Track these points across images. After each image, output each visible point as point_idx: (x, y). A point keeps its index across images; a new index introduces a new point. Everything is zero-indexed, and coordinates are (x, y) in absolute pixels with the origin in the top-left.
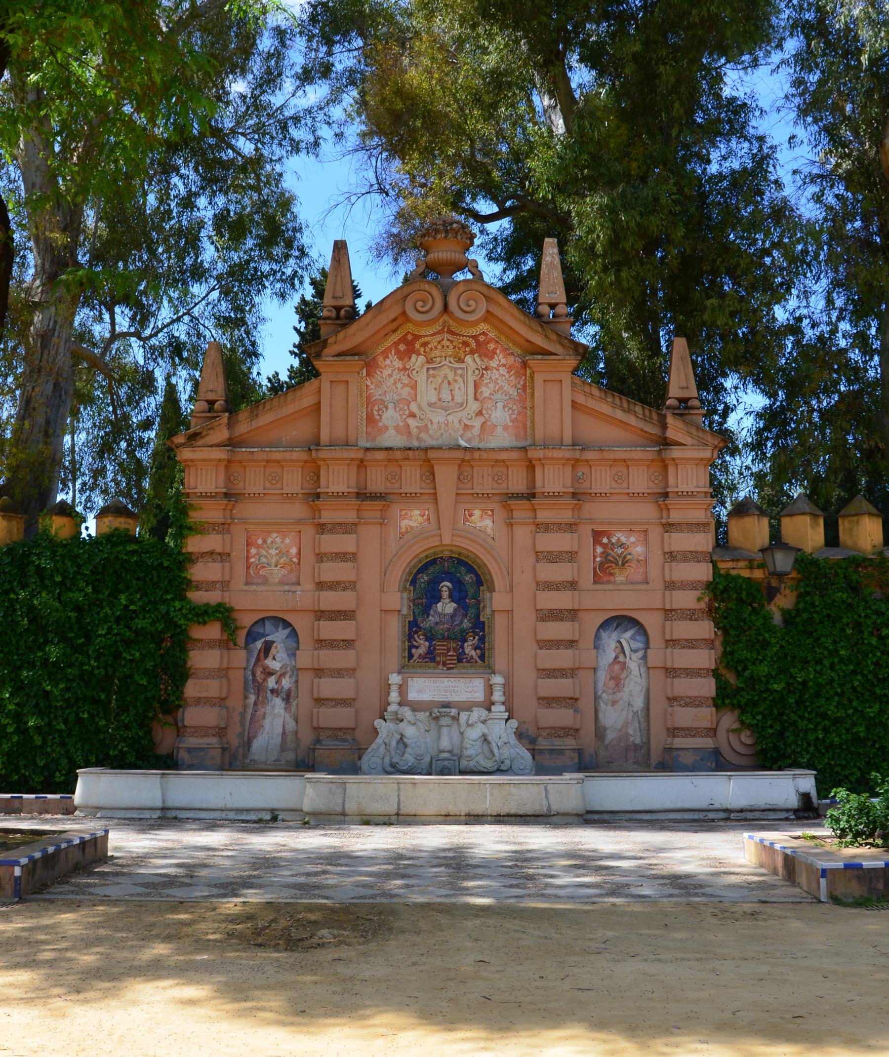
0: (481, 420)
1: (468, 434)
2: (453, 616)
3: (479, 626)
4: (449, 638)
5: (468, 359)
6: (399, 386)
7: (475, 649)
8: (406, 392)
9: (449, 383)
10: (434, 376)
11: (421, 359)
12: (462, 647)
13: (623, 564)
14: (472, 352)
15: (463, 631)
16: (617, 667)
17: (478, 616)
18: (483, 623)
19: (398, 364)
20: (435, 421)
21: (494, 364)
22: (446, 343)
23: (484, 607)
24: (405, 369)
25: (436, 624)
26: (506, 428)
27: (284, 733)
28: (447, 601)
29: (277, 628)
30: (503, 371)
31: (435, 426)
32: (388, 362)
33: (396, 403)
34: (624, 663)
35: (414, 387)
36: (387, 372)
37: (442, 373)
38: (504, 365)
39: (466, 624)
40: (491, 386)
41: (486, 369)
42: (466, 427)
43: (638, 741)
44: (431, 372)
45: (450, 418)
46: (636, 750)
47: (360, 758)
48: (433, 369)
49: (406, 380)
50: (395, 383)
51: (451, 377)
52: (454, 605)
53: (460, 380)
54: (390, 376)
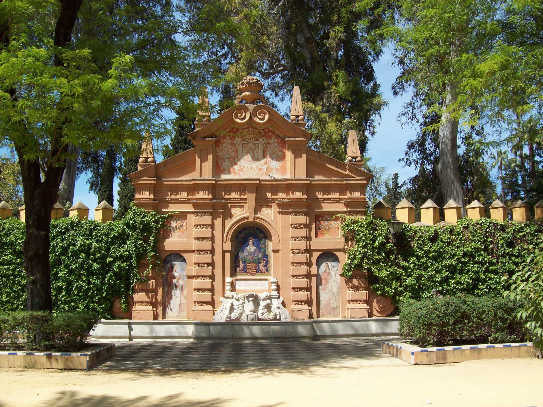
0: (266, 166)
1: (261, 173)
2: (254, 252)
3: (266, 257)
4: (252, 262)
5: (261, 139)
6: (230, 151)
7: (264, 267)
8: (233, 154)
9: (252, 150)
10: (245, 147)
11: (240, 139)
12: (258, 266)
13: (328, 229)
14: (262, 136)
15: (258, 259)
16: (326, 274)
17: (265, 252)
18: (267, 255)
19: (229, 141)
20: (246, 167)
21: (272, 141)
22: (250, 132)
23: (268, 248)
24: (233, 144)
25: (247, 256)
26: (277, 170)
27: (180, 304)
28: (252, 245)
29: (177, 258)
30: (276, 145)
31: (246, 169)
32: (225, 140)
33: (229, 159)
34: (329, 272)
35: (237, 151)
36: (225, 145)
37: (249, 145)
38: (276, 142)
39: (260, 256)
40: (271, 151)
41: (268, 144)
42: (260, 170)
43: (335, 306)
44: (244, 145)
45: (252, 165)
46: (334, 310)
47: (214, 315)
48: (245, 144)
49: (233, 148)
50: (228, 150)
51: (253, 147)
52: (255, 247)
53: (257, 148)
54: (226, 147)
